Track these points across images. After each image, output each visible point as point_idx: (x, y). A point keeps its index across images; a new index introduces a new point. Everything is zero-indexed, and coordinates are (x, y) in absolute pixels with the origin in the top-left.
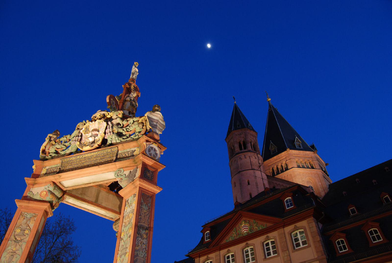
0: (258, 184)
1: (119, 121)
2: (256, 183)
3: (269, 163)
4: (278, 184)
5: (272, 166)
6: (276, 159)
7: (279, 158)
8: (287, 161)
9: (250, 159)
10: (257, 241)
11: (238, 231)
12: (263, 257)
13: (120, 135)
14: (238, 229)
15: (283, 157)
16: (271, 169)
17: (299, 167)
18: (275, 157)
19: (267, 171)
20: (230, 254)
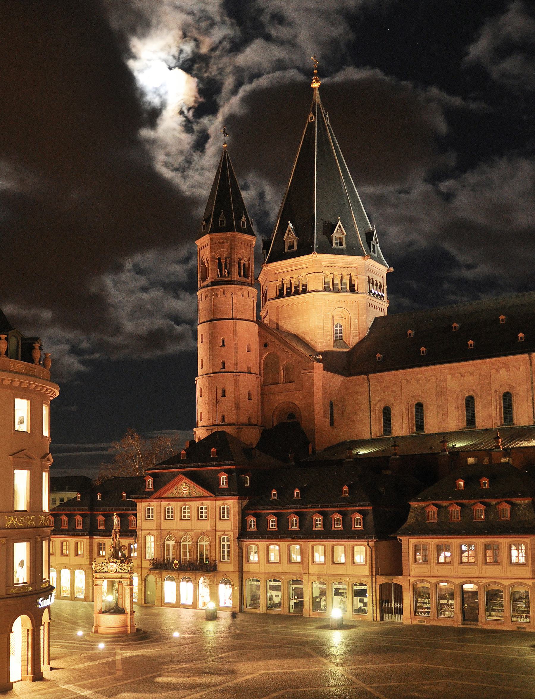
0: (239, 346)
1: (119, 564)
2: (236, 344)
3: (278, 269)
4: (272, 340)
5: (283, 276)
6: (291, 266)
7: (297, 265)
8: (309, 275)
9: (232, 298)
10: (194, 504)
11: (179, 491)
12: (197, 519)
13: (121, 569)
14: (179, 488)
15: (302, 264)
16: (280, 279)
17: (326, 289)
18: (290, 261)
19: (272, 283)
20: (170, 507)
